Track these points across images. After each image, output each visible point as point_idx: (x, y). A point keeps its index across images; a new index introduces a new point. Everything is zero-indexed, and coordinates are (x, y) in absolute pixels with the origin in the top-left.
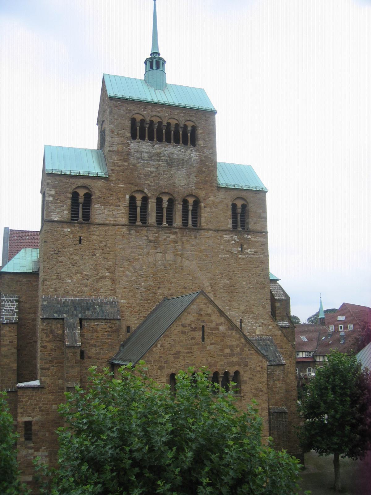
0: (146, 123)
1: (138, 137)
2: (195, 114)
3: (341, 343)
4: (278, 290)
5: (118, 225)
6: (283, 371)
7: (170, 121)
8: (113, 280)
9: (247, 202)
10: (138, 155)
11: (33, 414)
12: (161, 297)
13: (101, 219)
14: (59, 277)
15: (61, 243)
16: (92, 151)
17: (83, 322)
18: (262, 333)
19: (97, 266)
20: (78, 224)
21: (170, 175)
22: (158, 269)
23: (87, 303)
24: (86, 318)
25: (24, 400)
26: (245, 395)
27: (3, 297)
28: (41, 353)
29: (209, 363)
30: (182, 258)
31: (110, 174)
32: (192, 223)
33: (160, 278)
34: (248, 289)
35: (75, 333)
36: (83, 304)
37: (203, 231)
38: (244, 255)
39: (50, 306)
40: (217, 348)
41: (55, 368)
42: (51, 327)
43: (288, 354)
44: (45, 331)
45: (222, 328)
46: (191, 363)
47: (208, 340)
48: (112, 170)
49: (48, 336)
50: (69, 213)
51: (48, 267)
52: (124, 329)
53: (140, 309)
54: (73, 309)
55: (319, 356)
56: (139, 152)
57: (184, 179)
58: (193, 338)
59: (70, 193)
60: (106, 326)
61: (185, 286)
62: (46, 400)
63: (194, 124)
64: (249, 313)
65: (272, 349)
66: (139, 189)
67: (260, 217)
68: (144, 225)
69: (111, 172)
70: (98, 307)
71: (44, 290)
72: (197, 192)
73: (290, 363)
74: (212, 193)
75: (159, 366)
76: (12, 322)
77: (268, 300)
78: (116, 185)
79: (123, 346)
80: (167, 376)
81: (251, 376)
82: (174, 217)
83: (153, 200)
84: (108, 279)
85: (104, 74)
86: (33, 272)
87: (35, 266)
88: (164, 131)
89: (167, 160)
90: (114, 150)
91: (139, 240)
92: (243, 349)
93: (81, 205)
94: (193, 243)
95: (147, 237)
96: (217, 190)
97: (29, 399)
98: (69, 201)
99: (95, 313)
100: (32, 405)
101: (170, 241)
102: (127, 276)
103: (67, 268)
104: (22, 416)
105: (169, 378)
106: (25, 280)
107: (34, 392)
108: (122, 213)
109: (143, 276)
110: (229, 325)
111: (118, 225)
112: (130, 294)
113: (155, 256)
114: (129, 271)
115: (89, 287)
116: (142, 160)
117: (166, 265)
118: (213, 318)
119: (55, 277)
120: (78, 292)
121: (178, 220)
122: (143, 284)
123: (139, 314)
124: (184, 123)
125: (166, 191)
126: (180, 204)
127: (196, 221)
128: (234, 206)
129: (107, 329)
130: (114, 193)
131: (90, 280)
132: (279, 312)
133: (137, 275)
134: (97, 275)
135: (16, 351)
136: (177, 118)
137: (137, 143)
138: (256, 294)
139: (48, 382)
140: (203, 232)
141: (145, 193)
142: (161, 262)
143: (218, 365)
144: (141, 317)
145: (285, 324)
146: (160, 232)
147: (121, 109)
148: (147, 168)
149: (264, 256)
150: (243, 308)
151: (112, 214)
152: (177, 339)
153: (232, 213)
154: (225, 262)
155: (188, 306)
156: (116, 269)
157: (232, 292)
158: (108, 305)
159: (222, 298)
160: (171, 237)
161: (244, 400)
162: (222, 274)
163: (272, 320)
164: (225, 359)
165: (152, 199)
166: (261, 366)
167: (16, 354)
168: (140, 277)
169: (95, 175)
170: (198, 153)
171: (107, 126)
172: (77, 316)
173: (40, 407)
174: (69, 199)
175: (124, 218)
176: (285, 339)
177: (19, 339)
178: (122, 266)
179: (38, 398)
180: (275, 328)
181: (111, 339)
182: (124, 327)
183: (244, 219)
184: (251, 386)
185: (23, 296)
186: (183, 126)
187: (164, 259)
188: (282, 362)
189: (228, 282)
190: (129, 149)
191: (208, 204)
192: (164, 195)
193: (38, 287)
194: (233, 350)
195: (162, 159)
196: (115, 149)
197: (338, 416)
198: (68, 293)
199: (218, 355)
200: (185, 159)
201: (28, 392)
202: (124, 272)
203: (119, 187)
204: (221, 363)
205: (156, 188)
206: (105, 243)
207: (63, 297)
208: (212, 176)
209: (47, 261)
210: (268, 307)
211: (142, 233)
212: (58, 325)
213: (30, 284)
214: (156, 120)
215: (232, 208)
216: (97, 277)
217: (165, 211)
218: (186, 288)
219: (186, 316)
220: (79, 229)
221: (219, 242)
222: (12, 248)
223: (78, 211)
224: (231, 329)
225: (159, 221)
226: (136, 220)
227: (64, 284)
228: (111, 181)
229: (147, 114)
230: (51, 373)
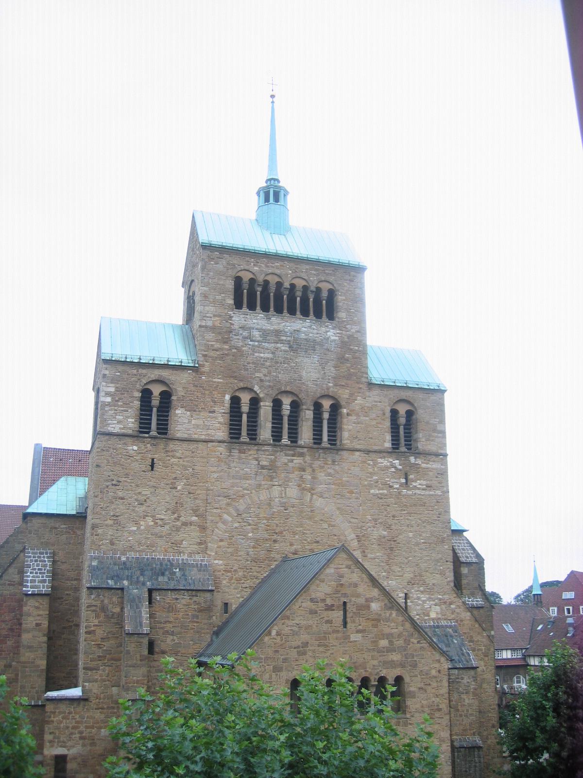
0: (259, 285)
1: (245, 305)
2: (333, 271)
3: (568, 635)
4: (464, 546)
5: (212, 441)
6: (475, 678)
7: (295, 281)
8: (203, 528)
9: (415, 407)
10: (245, 334)
11: (69, 744)
12: (278, 557)
13: (186, 432)
14: (117, 523)
15: (123, 469)
16: (173, 326)
17: (154, 595)
18: (440, 616)
19: (178, 505)
20: (150, 439)
21: (295, 364)
22: (274, 512)
23: (161, 564)
24: (159, 587)
25: (55, 719)
26: (412, 716)
27: (29, 553)
28: (85, 643)
29: (354, 663)
30: (312, 494)
31: (201, 363)
32: (329, 440)
33: (277, 525)
34: (417, 544)
35: (140, 612)
36: (154, 566)
37: (345, 451)
38: (411, 489)
39: (102, 568)
41: (107, 668)
42: (103, 601)
43: (482, 650)
44: (94, 608)
45: (374, 606)
47: (353, 625)
48: (205, 356)
49: (97, 616)
50: (136, 421)
51: (100, 506)
52: (219, 607)
53: (244, 575)
54: (139, 572)
55: (534, 656)
56: (247, 328)
57: (317, 371)
58: (329, 622)
59: (138, 391)
60: (188, 601)
61: (317, 539)
62: (92, 721)
63: (331, 287)
64: (418, 584)
65: (456, 642)
66: (245, 386)
67: (435, 430)
68: (253, 442)
69: (202, 359)
70: (178, 570)
71: (93, 542)
72: (336, 390)
73: (485, 666)
74: (360, 393)
75: (273, 666)
76: (41, 592)
77: (448, 563)
78: (210, 379)
79: (217, 633)
80: (286, 683)
81: (422, 685)
82: (300, 430)
83: (267, 404)
84: (196, 526)
85: (194, 210)
86: (78, 513)
87: (81, 504)
88: (285, 296)
89: (289, 341)
90: (207, 324)
91: (244, 466)
92: (409, 640)
93: (155, 410)
94: (329, 471)
95: (257, 460)
96: (367, 388)
97: (63, 718)
98: (137, 403)
99: (173, 580)
100: (68, 727)
101: (293, 467)
102: (225, 522)
103: (131, 508)
104: (52, 746)
106: (65, 526)
107: (73, 707)
108: (219, 423)
109: (250, 522)
110: (386, 601)
111: (212, 441)
112: (230, 550)
113: (269, 492)
114: (229, 514)
115: (164, 538)
116: (251, 341)
117: (287, 505)
118: (360, 590)
119: (110, 522)
120: (148, 546)
121: (306, 434)
122: (250, 535)
123: (243, 583)
124: (317, 284)
125: (288, 389)
126: (309, 410)
127: (335, 436)
128: (394, 413)
129: (193, 606)
130: (207, 392)
131: (167, 527)
132: (467, 583)
133: (241, 520)
134: (177, 519)
135: (45, 639)
136: (306, 278)
137: (245, 314)
138: (430, 552)
139: (95, 691)
140: (345, 454)
141: (255, 392)
142: (280, 501)
143: (368, 666)
144: (247, 588)
145: (477, 601)
146: (278, 454)
147: (220, 263)
148: (258, 353)
149: (442, 492)
150: (410, 575)
151: (202, 423)
152: (303, 623)
153: (391, 424)
154: (381, 501)
155: (320, 570)
156: (208, 511)
157: (391, 549)
158: (194, 567)
159: (375, 558)
160: (295, 461)
161: (410, 724)
162: (375, 520)
163: (455, 595)
164: (380, 656)
165: (265, 401)
166: (438, 669)
167: (46, 645)
168: (245, 524)
169: (177, 364)
170: (338, 331)
171: (198, 289)
172: (144, 584)
173: (81, 733)
174: (137, 400)
175: (221, 431)
176: (477, 626)
177: (52, 619)
178: (217, 505)
179: (77, 716)
180: (460, 608)
181: (198, 622)
182: (219, 604)
183: (410, 433)
184: (423, 702)
185: (60, 551)
186: (315, 290)
187: (283, 495)
188: (472, 664)
189: (385, 533)
190: (232, 324)
191: (354, 410)
192: (285, 396)
193: (84, 538)
195: (282, 340)
196: (210, 323)
197: (564, 754)
198: (131, 548)
199: (369, 650)
200: (318, 340)
201: (63, 707)
202: (220, 516)
203: (215, 382)
204: (374, 664)
205: (271, 384)
206: (191, 470)
207: (124, 553)
208: (359, 366)
209: (100, 497)
210: (448, 573)
211: (250, 455)
212: (115, 599)
213: (72, 533)
214: (273, 280)
215: (391, 416)
216: (179, 523)
217: (285, 420)
218: (318, 542)
219: (317, 586)
220: (151, 448)
221: (371, 470)
222: (46, 476)
223: (151, 420)
224: (390, 608)
225: (277, 435)
226: (240, 434)
227: (126, 534)
228: (202, 373)
229: (260, 271)
230: (101, 676)
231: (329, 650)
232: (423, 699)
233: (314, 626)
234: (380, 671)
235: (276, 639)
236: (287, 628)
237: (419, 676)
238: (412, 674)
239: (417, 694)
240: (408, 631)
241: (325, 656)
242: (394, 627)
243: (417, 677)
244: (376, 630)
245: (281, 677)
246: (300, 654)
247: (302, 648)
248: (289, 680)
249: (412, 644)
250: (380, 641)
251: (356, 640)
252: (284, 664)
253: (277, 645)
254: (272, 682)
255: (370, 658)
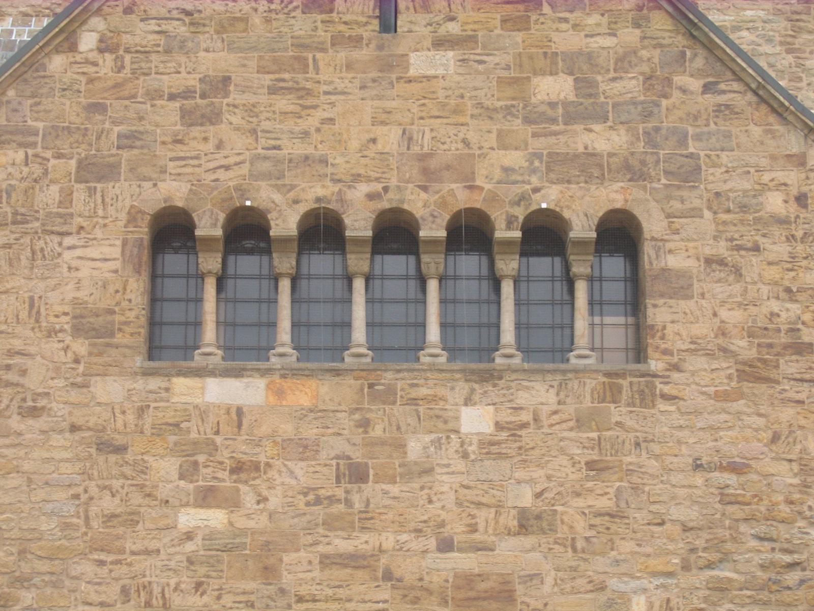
26: (676, 368)
29: (422, 158)
40: (481, 67)
46: (299, 149)
47: (422, 18)
75: (80, 162)
80: (133, 217)
81: (722, 249)
92: (669, 81)
105: (143, 232)
161: (664, 397)
164: (534, 135)
166: (794, 192)
184: (724, 314)
194: (592, 84)
199: (489, 113)
231: (315, 107)
232: (723, 303)
233: (257, 20)
234: (536, 190)
235: (95, 64)
236: (142, 25)
237: (707, 214)
238: (677, 205)
239: (696, 285)
240: (661, 46)
241: (297, 129)
242: (600, 31)
243: (702, 217)
244: (519, 40)
245: (108, 200)
246: (189, 117)
247: (203, 96)
248: (143, 213)
249: (676, 94)
250: (535, 80)
251: (431, 72)
252: (125, 154)
253: (99, 85)
254: (71, 215)
255: (492, 140)
